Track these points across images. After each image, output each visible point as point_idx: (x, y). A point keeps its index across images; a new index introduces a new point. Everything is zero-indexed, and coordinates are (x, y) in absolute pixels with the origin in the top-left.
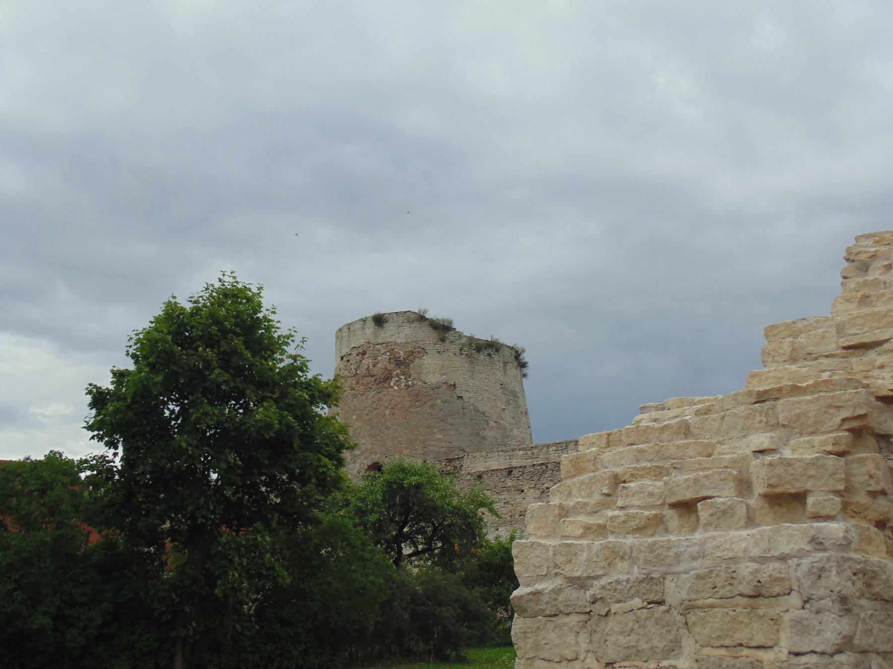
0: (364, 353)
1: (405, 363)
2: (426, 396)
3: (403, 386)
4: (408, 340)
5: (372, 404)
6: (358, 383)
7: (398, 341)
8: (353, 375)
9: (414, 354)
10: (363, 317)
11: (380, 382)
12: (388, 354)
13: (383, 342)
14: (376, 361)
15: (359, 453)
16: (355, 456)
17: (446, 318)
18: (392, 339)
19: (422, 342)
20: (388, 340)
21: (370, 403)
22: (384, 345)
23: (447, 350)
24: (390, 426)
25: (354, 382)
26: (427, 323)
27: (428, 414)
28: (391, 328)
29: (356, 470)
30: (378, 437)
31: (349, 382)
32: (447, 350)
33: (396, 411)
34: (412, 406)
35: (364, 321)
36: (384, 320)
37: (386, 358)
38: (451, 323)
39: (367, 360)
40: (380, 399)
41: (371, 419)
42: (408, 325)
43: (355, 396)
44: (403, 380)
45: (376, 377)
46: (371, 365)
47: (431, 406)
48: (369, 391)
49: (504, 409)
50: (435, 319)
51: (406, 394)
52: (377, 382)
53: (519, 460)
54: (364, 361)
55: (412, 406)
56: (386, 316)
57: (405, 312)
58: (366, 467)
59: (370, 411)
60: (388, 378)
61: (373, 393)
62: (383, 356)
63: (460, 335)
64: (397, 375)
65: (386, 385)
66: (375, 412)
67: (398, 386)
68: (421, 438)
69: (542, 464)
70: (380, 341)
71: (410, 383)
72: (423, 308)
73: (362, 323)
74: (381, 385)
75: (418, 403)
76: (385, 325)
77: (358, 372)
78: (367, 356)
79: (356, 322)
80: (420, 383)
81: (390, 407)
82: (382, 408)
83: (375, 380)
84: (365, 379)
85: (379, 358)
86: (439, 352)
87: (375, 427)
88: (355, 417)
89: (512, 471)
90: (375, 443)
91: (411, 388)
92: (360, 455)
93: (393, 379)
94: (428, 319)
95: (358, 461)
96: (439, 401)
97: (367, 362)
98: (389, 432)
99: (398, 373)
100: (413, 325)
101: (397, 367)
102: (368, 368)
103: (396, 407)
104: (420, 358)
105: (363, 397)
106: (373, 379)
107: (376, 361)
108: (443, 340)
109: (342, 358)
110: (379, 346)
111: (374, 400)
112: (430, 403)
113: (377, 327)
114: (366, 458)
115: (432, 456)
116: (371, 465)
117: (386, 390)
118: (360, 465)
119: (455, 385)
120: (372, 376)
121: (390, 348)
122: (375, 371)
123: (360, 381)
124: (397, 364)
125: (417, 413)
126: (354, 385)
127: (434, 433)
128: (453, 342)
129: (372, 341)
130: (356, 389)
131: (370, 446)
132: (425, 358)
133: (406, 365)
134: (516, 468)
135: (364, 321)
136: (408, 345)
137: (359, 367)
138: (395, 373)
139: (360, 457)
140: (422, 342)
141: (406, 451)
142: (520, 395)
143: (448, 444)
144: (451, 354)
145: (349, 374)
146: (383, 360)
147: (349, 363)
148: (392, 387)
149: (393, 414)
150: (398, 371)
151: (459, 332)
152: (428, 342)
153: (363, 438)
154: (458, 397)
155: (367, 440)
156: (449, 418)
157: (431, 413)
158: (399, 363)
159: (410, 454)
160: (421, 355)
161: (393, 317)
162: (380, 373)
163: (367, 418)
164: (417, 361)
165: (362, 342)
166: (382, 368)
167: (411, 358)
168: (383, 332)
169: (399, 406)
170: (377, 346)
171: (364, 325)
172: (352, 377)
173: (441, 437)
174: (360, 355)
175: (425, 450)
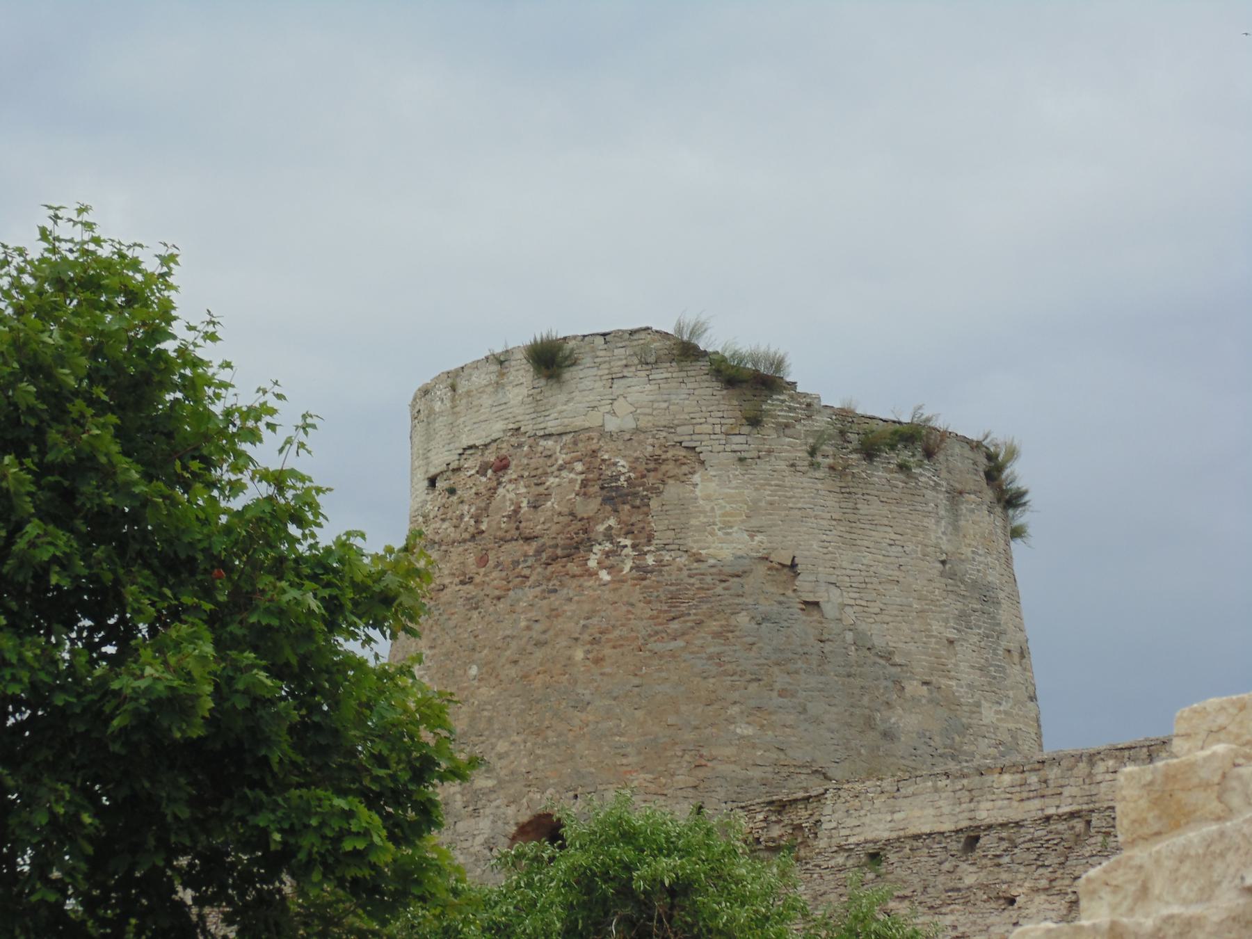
0: (502, 466)
1: (635, 494)
2: (702, 600)
3: (627, 569)
4: (643, 423)
5: (528, 628)
6: (482, 561)
7: (612, 425)
8: (466, 536)
9: (664, 468)
10: (498, 350)
11: (555, 558)
12: (579, 467)
13: (561, 429)
14: (541, 489)
15: (490, 783)
16: (477, 794)
17: (763, 349)
18: (594, 420)
19: (688, 429)
20: (579, 422)
21: (523, 624)
22: (565, 438)
23: (770, 452)
24: (588, 698)
25: (471, 559)
26: (703, 365)
27: (710, 658)
28: (587, 383)
29: (480, 840)
30: (549, 733)
31: (454, 557)
32: (770, 452)
33: (607, 651)
34: (657, 633)
35: (501, 363)
36: (566, 358)
37: (572, 481)
38: (779, 364)
39: (511, 487)
40: (554, 614)
41: (525, 677)
42: (644, 374)
43: (474, 604)
44: (628, 551)
45: (541, 541)
46: (524, 504)
47: (717, 635)
48: (520, 586)
49: (951, 642)
50: (727, 355)
51: (637, 595)
52: (544, 556)
53: (999, 803)
54: (501, 491)
55: (657, 633)
56: (571, 344)
57: (632, 333)
58: (513, 829)
59: (522, 651)
60: (578, 546)
61: (531, 593)
62: (564, 473)
63: (809, 405)
64: (608, 535)
65: (573, 568)
66: (539, 654)
67: (610, 569)
68: (689, 736)
69: (1073, 815)
70: (552, 425)
71: (650, 560)
72: (690, 319)
73: (495, 368)
74: (556, 567)
75: (675, 625)
76: (567, 375)
77: (483, 527)
78: (512, 474)
79: (476, 365)
80: (683, 560)
81: (586, 637)
82: (563, 642)
83: (538, 552)
84: (507, 547)
85: (552, 481)
86: (741, 460)
87: (538, 702)
88: (474, 671)
89: (977, 839)
90: (539, 752)
91: (653, 577)
92: (492, 790)
93: (596, 548)
94: (705, 353)
95: (488, 811)
96: (743, 619)
97: (511, 493)
98: (583, 716)
99: (610, 528)
100: (657, 375)
101: (608, 508)
102: (516, 512)
103: (604, 638)
104: (682, 480)
105: (501, 605)
106: (531, 549)
107: (541, 489)
108: (755, 422)
109: (432, 482)
110: (550, 443)
111: (533, 615)
112: (714, 625)
113: (543, 382)
115: (721, 794)
116: (530, 823)
117: (575, 582)
118: (494, 822)
119: (793, 566)
120: (527, 539)
122: (537, 523)
123: (491, 555)
124: (607, 500)
125: (673, 655)
126: (472, 568)
127: (731, 721)
128: (787, 426)
129: (528, 427)
130: (478, 579)
131: (525, 761)
132: (696, 478)
133: (638, 502)
134: (990, 827)
135: (501, 363)
136: (642, 436)
137: (486, 509)
138: (601, 528)
139: (493, 796)
140: (688, 429)
141: (639, 779)
142: (1002, 595)
143: (774, 755)
144: (782, 465)
145: (454, 534)
147: (454, 498)
148: (592, 574)
149: (598, 661)
150: (612, 522)
151: (806, 395)
152: (707, 428)
153: (500, 737)
154: (806, 603)
155: (513, 743)
156: (776, 669)
157: (719, 655)
158: (614, 496)
159: (652, 787)
160: (685, 469)
161: (593, 350)
162: (555, 528)
163: (513, 672)
164: (672, 490)
165: (497, 428)
166: (560, 514)
167: (651, 480)
168: (563, 397)
169: (616, 633)
170: (543, 443)
171: (502, 375)
172: (465, 541)
173: (749, 731)
174: (490, 472)
175: (700, 773)
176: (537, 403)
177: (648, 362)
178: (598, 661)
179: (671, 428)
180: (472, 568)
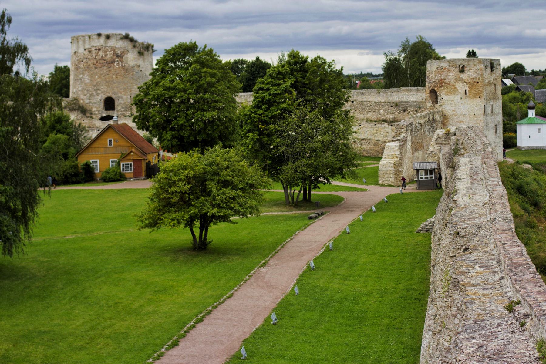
0: (99, 50)
6: (97, 62)
20: (112, 45)
33: (118, 76)
40: (110, 71)
43: (96, 68)
54: (99, 53)
60: (113, 62)
64: (117, 61)
66: (108, 76)
68: (129, 88)
70: (108, 45)
71: (123, 65)
78: (101, 51)
82: (111, 75)
100: (123, 40)
104: (127, 54)
110: (107, 48)
114: (104, 94)
121: (113, 49)
122: (106, 58)
126: (95, 63)
129: (104, 45)
141: (123, 93)
146: (110, 54)
149: (117, 77)
158: (118, 56)
163: (103, 78)
164: (126, 56)
165: (98, 44)
176: (106, 42)
177: (121, 39)
178: (117, 77)
179: (125, 47)
180: (95, 63)
